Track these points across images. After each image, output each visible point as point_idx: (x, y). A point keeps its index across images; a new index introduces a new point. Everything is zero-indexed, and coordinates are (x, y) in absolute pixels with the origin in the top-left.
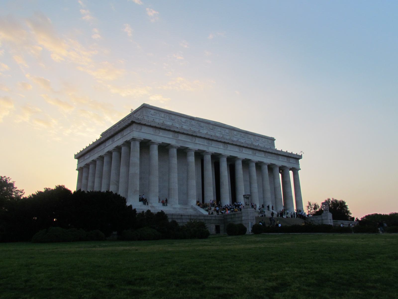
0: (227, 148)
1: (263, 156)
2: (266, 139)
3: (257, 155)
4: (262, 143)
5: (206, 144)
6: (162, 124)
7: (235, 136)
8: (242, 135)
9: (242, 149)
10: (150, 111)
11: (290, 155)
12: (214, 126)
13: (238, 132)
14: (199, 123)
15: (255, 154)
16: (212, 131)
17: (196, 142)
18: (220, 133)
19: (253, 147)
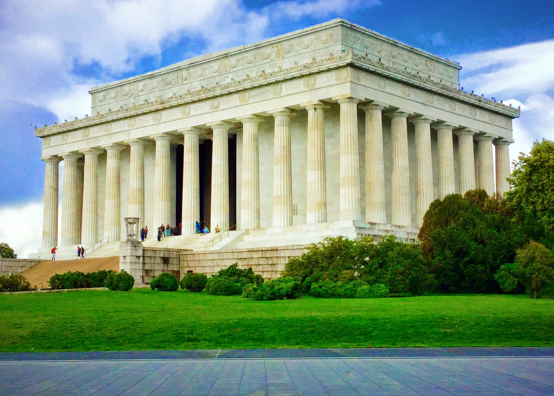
0: (160, 120)
1: (238, 103)
2: (313, 37)
3: (221, 107)
4: (300, 52)
5: (127, 128)
6: (64, 124)
7: (232, 70)
8: (247, 57)
9: (190, 109)
10: (99, 97)
11: (306, 72)
12: (191, 70)
13: (238, 57)
14: (165, 76)
15: (219, 106)
16: (186, 82)
17: (112, 132)
18: (201, 78)
19: (204, 95)
